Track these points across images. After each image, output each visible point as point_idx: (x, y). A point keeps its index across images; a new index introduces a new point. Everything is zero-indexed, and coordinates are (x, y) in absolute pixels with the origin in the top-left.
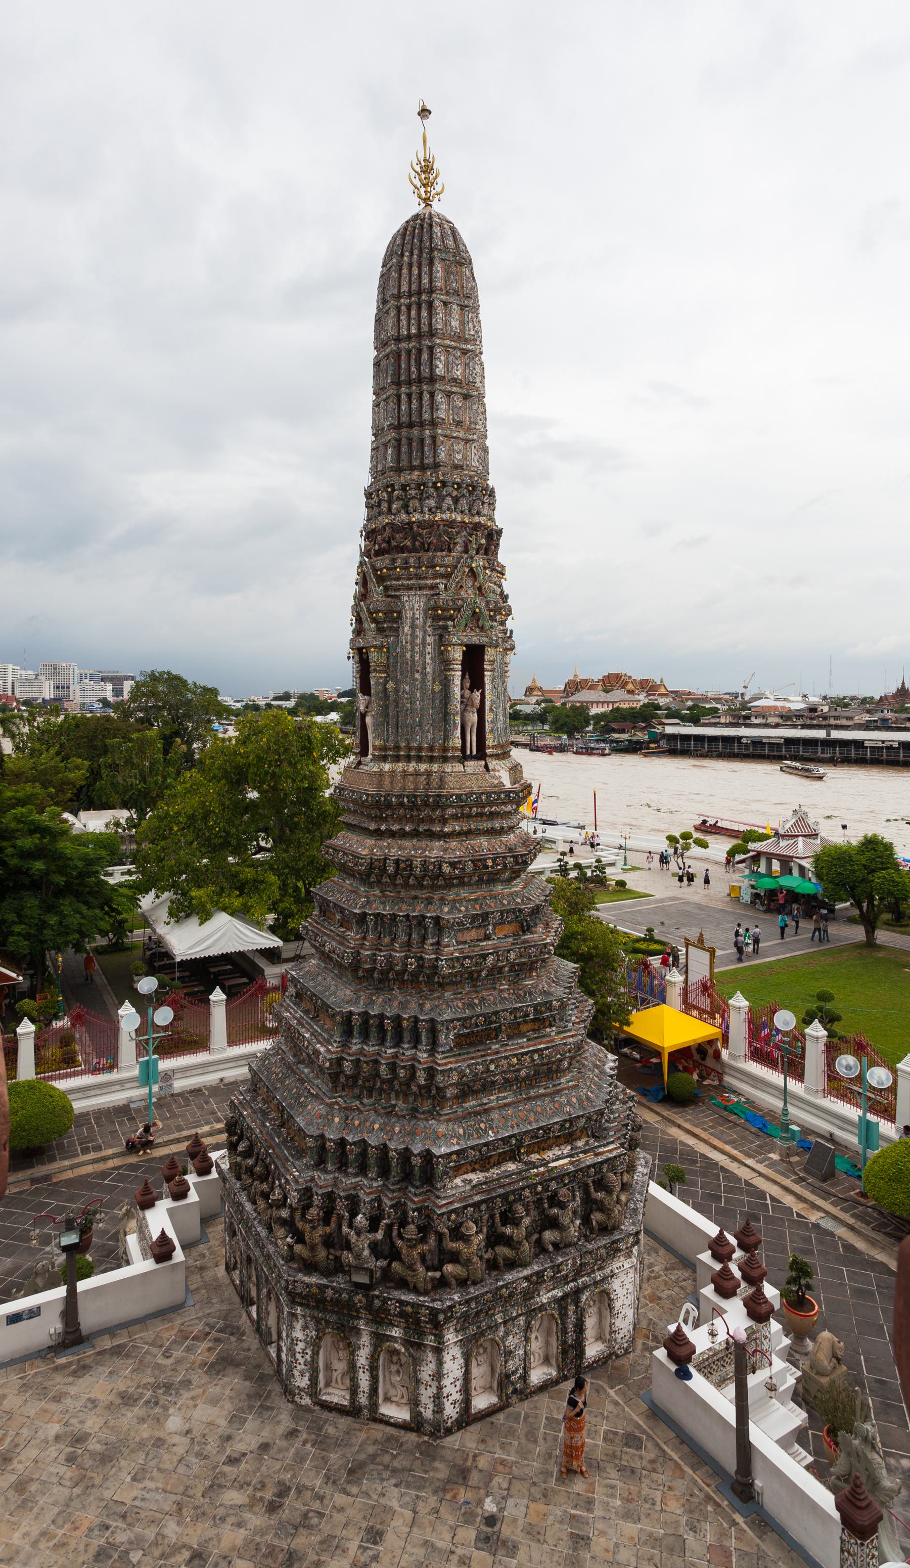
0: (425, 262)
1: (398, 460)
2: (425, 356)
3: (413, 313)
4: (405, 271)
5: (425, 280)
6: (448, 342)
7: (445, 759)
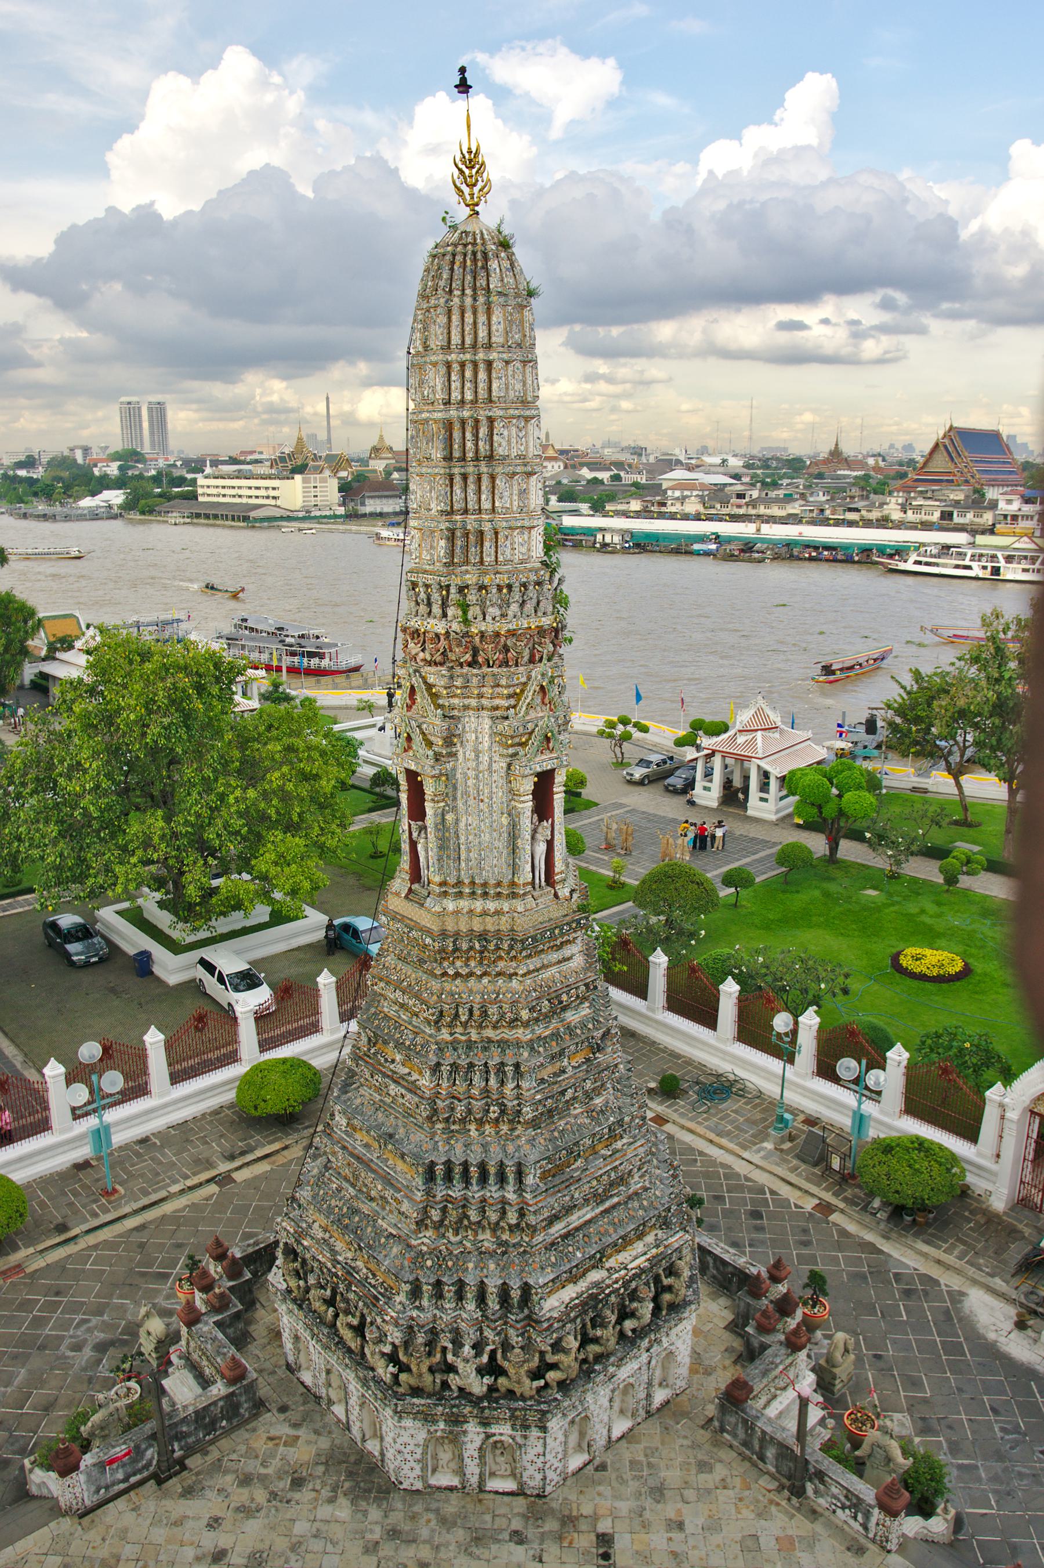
0: (481, 310)
1: (452, 554)
2: (483, 431)
3: (468, 374)
4: (455, 318)
5: (482, 333)
6: (511, 412)
7: (514, 895)
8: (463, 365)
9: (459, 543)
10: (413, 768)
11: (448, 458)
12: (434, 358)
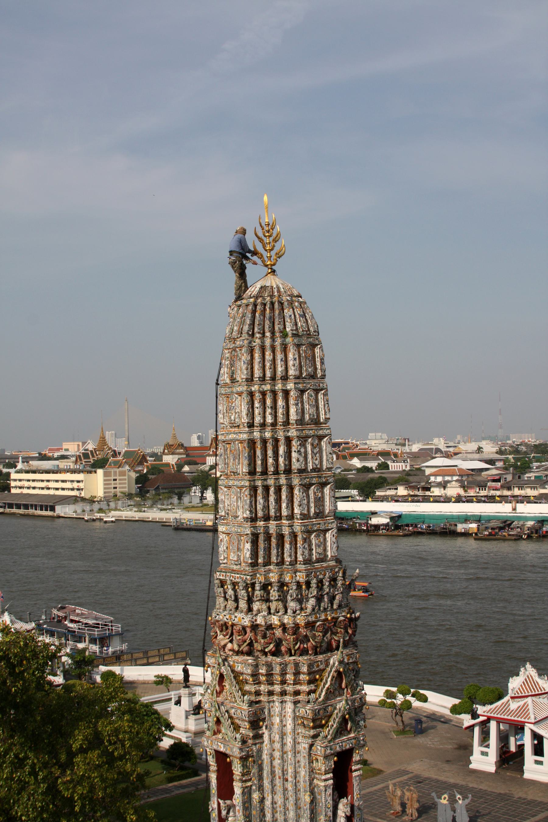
0: (278, 349)
3: (269, 402)
4: (257, 356)
5: (280, 369)
8: (264, 394)
9: (262, 545)
10: (222, 749)
11: (252, 472)
12: (240, 389)
